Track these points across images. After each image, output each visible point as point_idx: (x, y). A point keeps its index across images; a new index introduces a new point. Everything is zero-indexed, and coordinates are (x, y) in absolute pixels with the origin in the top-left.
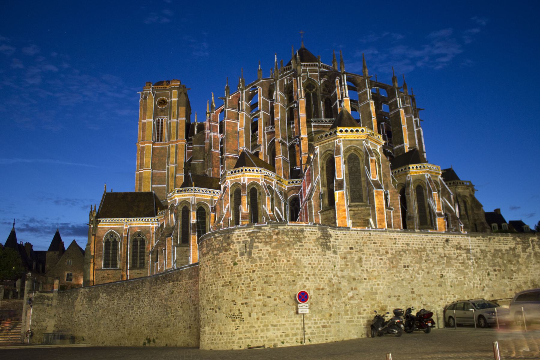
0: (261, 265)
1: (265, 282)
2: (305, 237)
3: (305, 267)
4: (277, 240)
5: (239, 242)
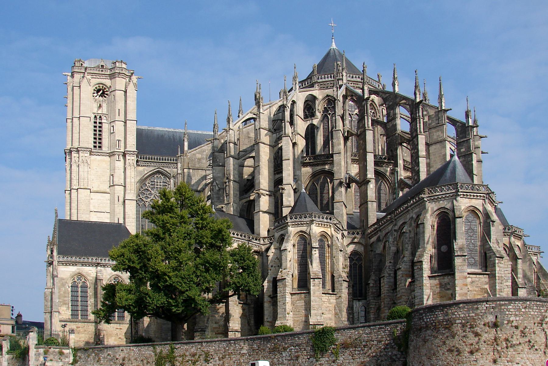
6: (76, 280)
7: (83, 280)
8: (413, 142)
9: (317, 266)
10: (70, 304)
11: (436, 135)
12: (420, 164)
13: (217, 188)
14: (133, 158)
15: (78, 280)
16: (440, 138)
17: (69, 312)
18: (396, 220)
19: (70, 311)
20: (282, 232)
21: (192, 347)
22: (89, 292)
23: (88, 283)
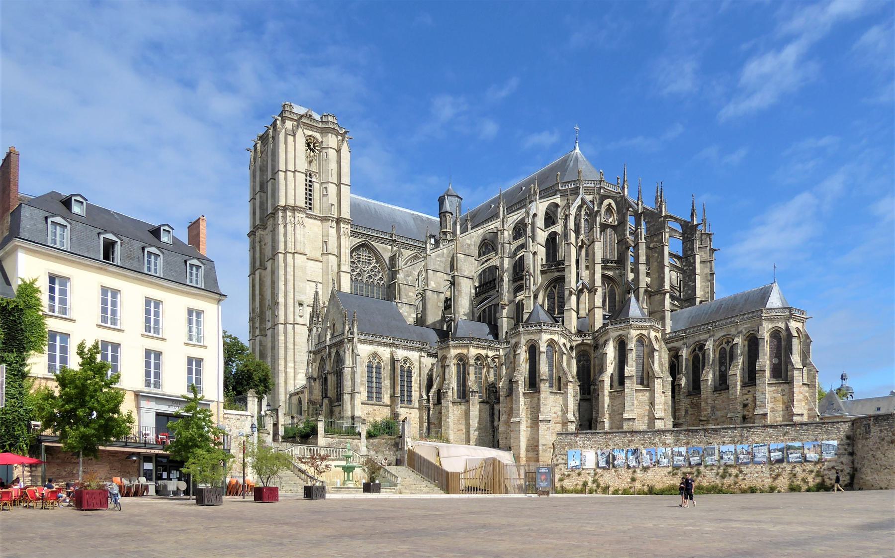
7: (378, 360)
14: (347, 226)
17: (366, 394)
21: (616, 436)
22: (383, 373)
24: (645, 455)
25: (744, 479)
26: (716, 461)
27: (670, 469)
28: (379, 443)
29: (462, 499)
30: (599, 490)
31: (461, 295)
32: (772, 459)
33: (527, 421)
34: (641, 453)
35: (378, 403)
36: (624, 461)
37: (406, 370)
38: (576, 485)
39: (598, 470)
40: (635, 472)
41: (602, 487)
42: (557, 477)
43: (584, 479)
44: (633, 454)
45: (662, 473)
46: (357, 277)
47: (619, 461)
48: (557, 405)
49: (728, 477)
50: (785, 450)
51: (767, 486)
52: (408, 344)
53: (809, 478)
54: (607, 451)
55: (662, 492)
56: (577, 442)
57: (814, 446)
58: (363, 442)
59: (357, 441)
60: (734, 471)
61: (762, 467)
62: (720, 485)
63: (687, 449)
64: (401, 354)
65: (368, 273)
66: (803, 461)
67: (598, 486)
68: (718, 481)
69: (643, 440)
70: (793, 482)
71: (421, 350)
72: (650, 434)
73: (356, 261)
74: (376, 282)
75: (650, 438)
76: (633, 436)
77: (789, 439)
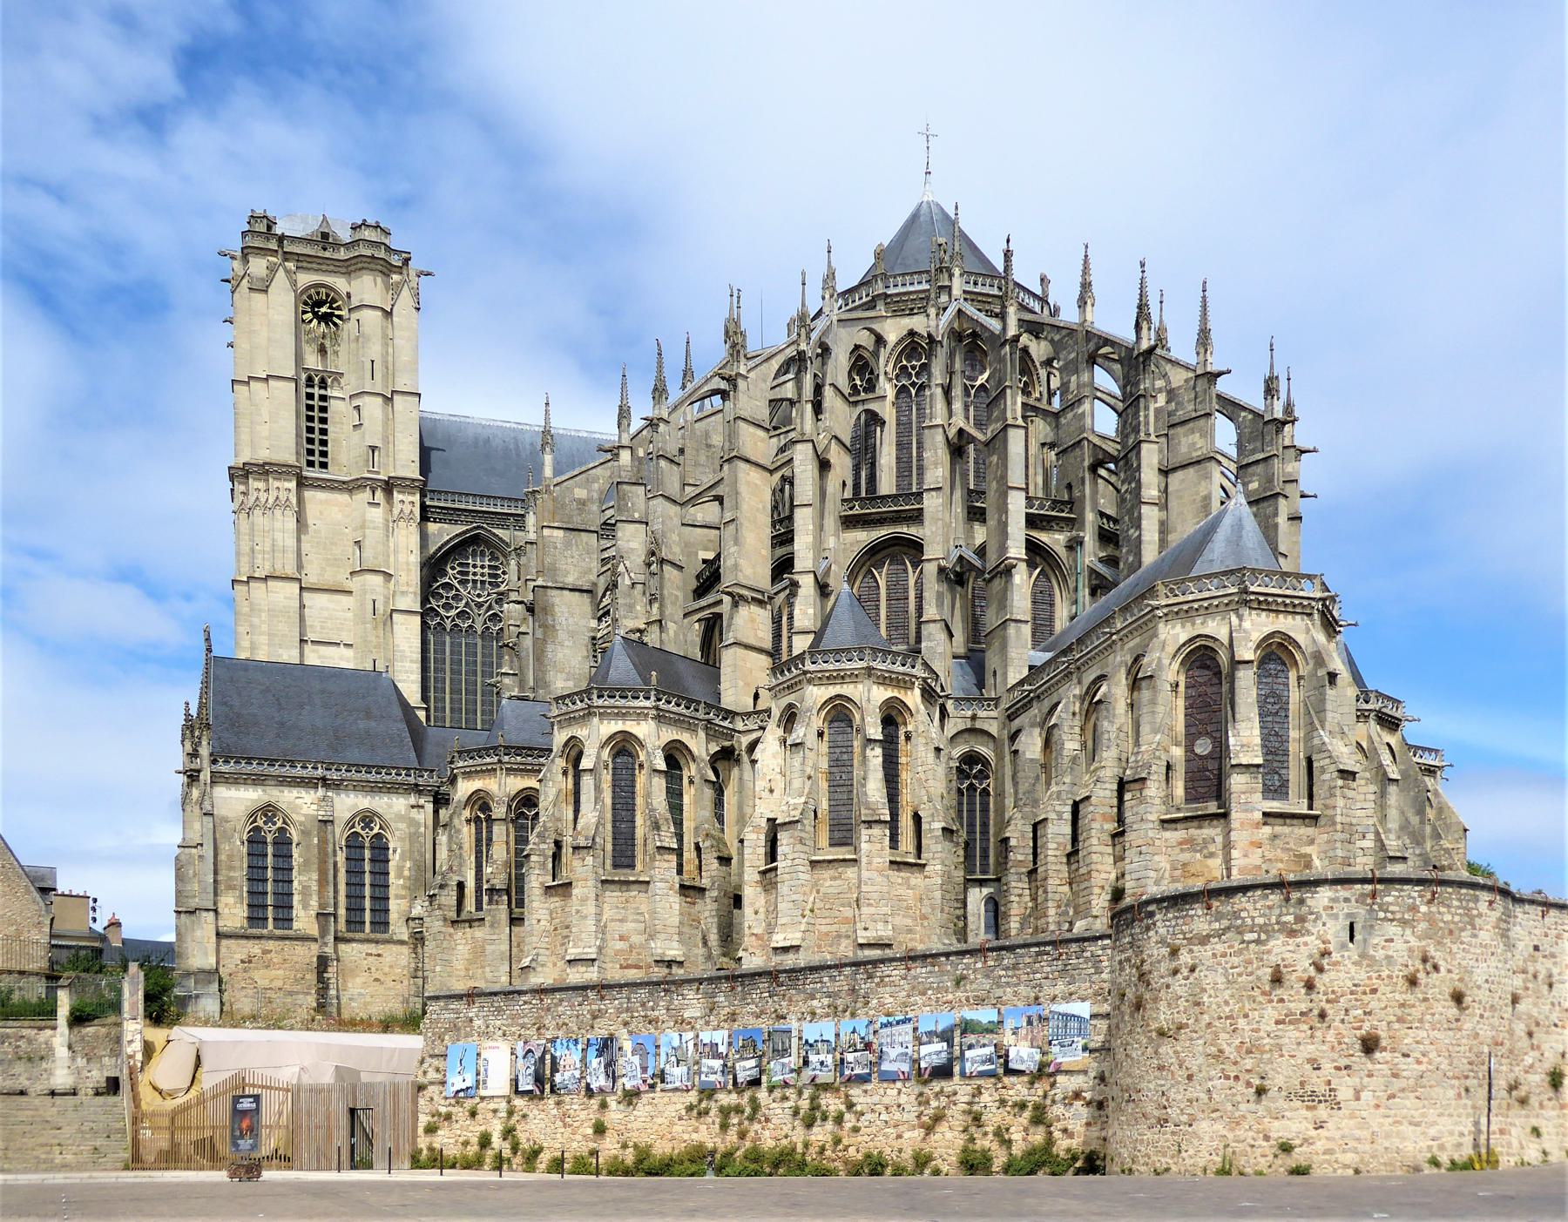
0: (1390, 977)
1: (1400, 1020)
2: (1480, 915)
3: (1479, 987)
4: (1429, 918)
5: (1336, 917)
6: (260, 823)
7: (279, 824)
8: (1127, 463)
9: (878, 790)
10: (245, 889)
11: (1189, 443)
12: (1144, 523)
13: (628, 582)
14: (411, 498)
15: (265, 823)
16: (1196, 450)
18: (1079, 668)
19: (245, 907)
20: (790, 699)
21: (561, 1000)
22: (295, 855)
23: (293, 831)
24: (629, 1054)
25: (856, 1130)
26: (792, 1071)
27: (692, 1097)
28: (96, 1036)
29: (202, 1185)
30: (518, 1160)
31: (555, 637)
32: (923, 1065)
33: (555, 965)
34: (620, 1049)
35: (278, 932)
36: (577, 1074)
37: (367, 845)
38: (466, 1143)
39: (519, 1102)
40: (604, 1105)
41: (524, 1151)
42: (424, 1120)
43: (483, 1128)
44: (600, 1053)
45: (672, 1108)
46: (458, 621)
47: (567, 1075)
48: (630, 918)
49: (819, 1122)
50: (957, 1033)
51: (908, 1154)
52: (370, 777)
53: (1012, 1129)
54: (537, 1044)
55: (665, 1168)
56: (471, 1020)
57: (1030, 1023)
58: (62, 1035)
59: (49, 1032)
60: (831, 1103)
61: (900, 1092)
62: (800, 1149)
63: (730, 1036)
64: (347, 804)
65: (490, 608)
66: (1001, 1071)
67: (515, 1149)
68: (798, 1136)
69: (627, 1010)
70: (972, 1140)
71: (416, 789)
72: (643, 993)
73: (455, 583)
74: (448, 624)
75: (643, 1005)
76: (602, 998)
77: (967, 999)
